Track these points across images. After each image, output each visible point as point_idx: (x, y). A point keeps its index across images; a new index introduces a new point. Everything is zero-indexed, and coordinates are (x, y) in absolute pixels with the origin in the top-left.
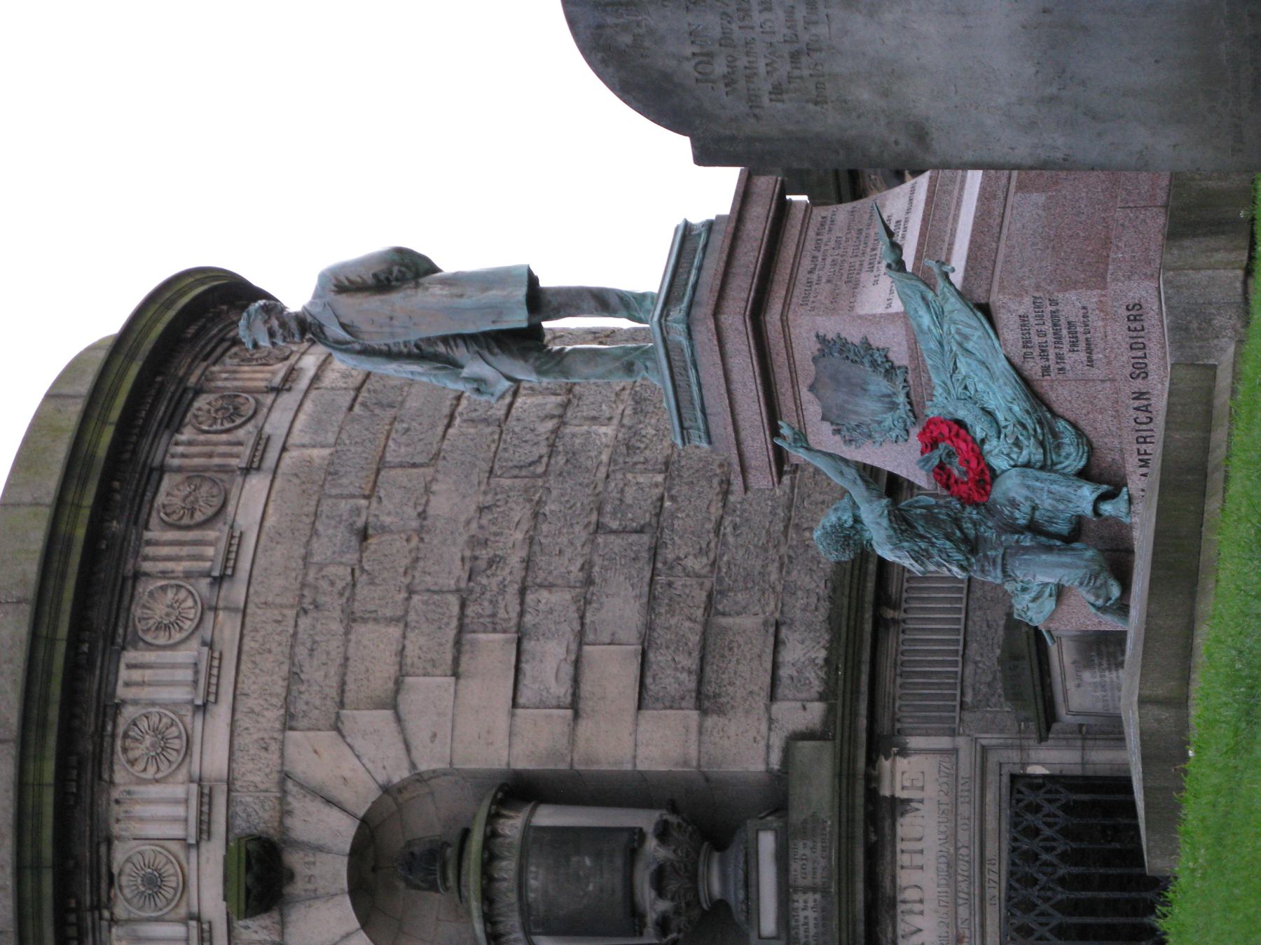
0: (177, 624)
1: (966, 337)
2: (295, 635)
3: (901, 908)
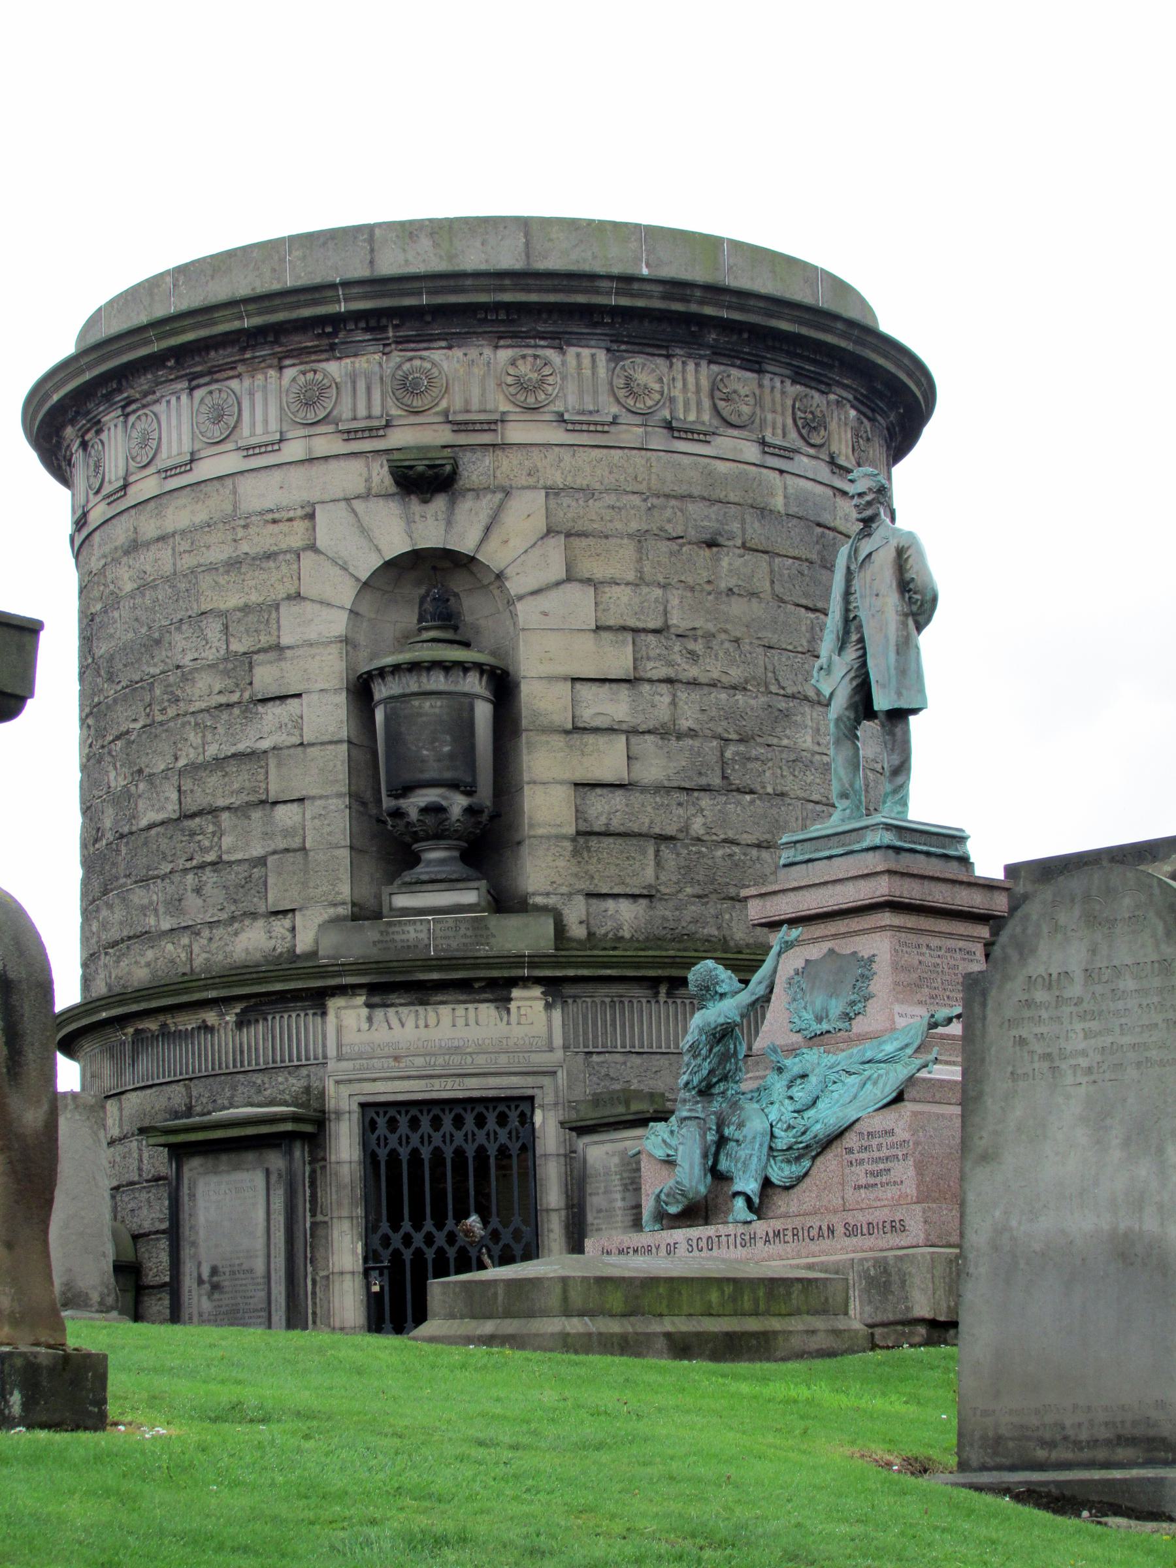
0: (632, 393)
1: (875, 1083)
2: (627, 492)
3: (420, 1009)
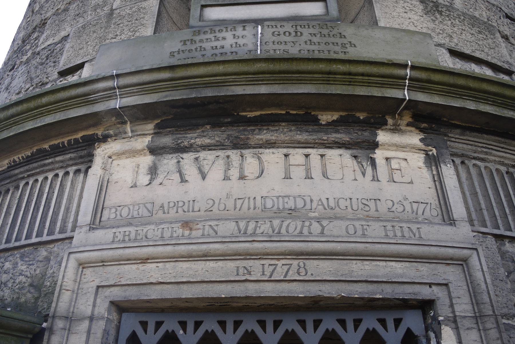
3: (234, 154)
